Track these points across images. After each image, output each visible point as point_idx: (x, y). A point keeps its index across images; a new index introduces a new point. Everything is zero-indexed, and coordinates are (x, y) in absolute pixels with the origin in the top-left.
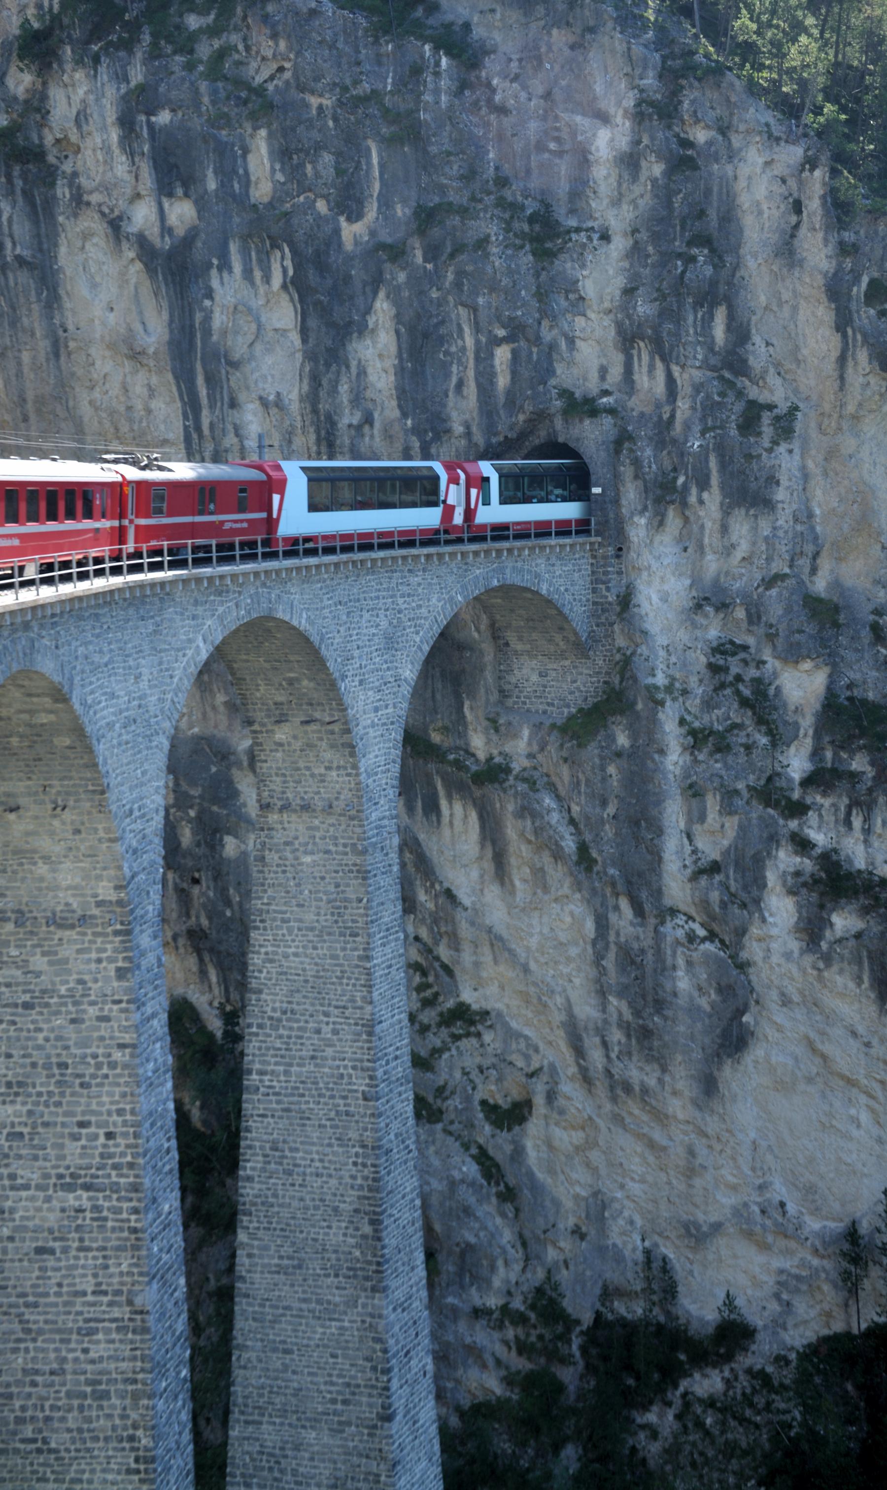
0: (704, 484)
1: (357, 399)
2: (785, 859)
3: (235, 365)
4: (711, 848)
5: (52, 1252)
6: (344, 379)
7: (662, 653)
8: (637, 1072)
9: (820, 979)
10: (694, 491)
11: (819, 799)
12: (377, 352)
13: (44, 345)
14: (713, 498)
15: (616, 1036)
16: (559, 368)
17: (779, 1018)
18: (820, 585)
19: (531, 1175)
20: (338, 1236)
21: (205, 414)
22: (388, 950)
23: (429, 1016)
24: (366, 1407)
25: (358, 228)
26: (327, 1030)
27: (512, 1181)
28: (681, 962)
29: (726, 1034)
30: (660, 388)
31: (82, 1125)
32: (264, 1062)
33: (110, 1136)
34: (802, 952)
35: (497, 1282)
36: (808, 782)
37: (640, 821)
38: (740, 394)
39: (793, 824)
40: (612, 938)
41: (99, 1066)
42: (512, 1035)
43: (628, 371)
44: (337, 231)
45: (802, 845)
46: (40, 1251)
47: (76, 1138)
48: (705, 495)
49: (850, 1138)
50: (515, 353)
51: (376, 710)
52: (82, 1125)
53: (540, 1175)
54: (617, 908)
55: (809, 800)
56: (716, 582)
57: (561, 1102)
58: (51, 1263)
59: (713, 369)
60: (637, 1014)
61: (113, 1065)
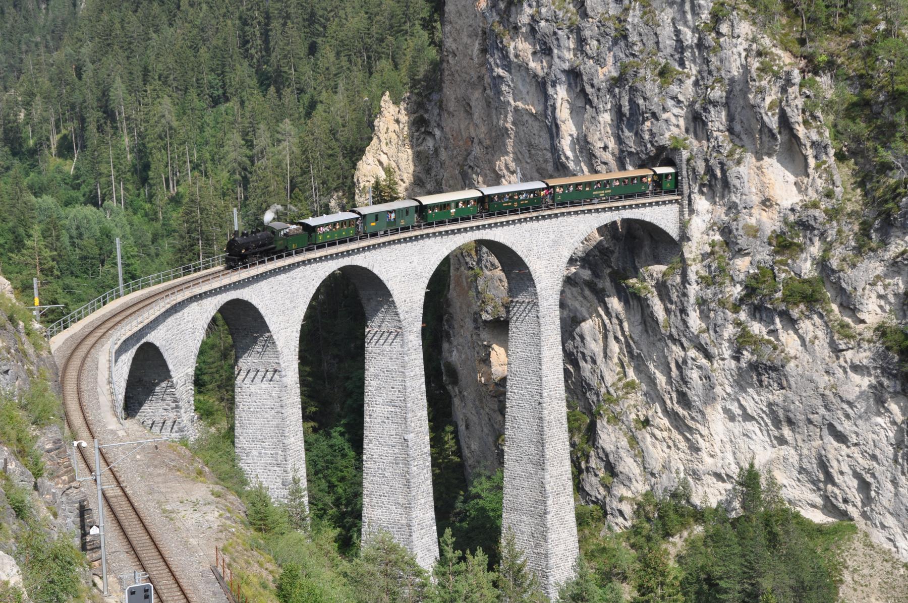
15: (674, 395)
16: (672, 128)
18: (753, 221)
19: (647, 448)
20: (532, 449)
23: (620, 384)
25: (605, 69)
35: (633, 488)
44: (597, 71)
50: (652, 123)
51: (547, 267)
53: (650, 447)
59: (722, 131)
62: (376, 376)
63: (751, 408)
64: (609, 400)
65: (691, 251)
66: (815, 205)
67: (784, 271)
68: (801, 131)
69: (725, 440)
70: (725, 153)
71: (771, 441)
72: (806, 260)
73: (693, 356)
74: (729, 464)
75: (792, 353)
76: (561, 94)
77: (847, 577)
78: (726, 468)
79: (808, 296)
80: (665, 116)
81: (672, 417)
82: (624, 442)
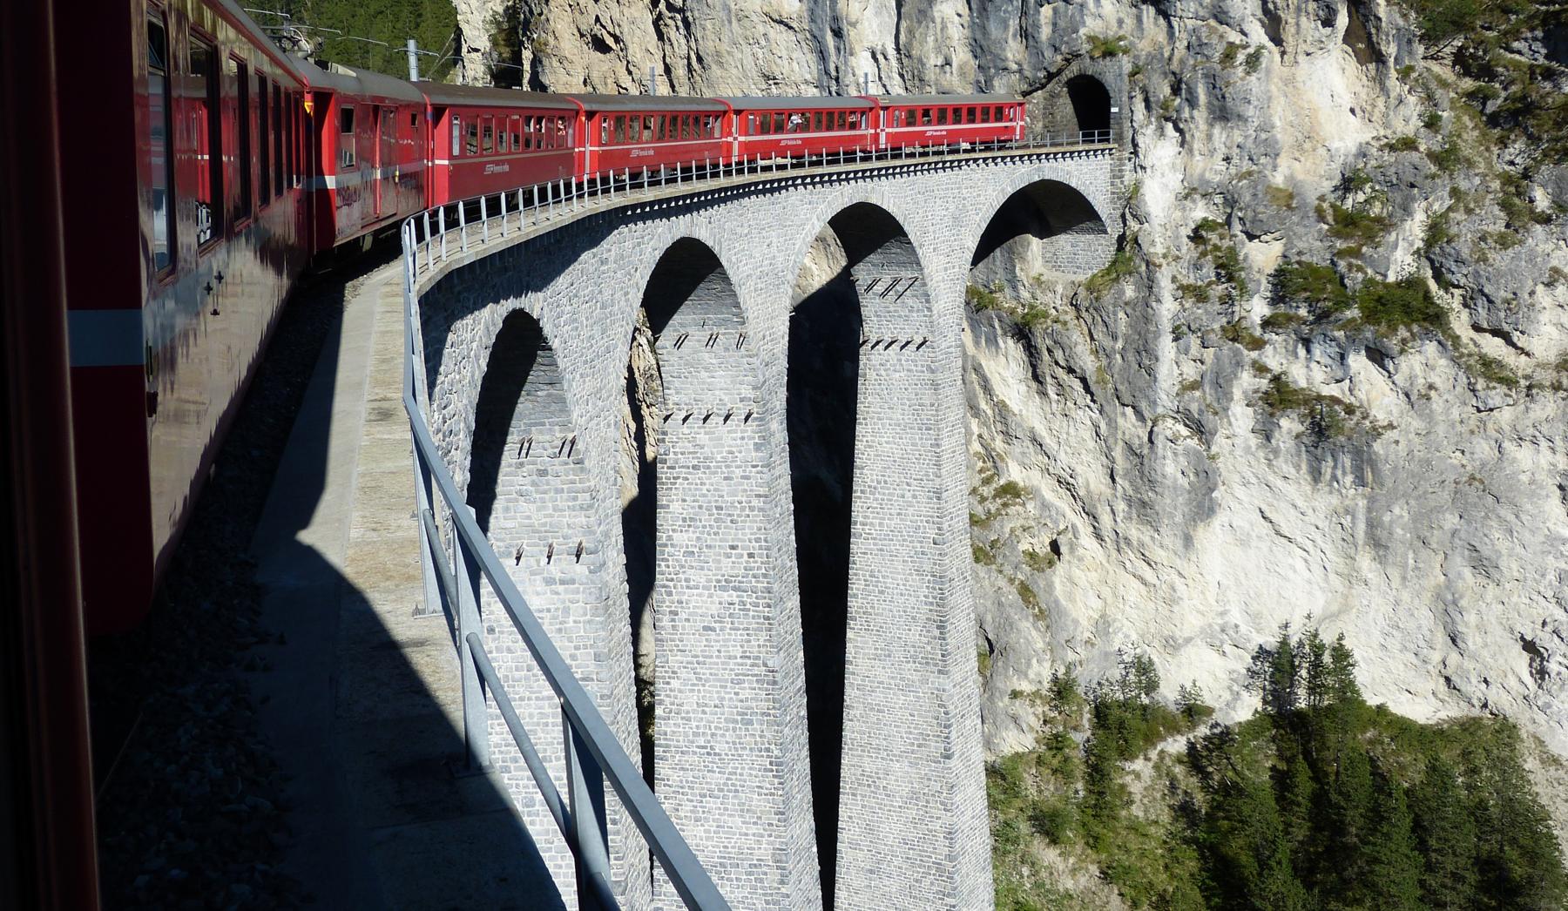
0: (1192, 102)
1: (942, 44)
2: (1246, 381)
3: (854, 25)
4: (1191, 371)
5: (713, 630)
6: (931, 32)
7: (1159, 229)
8: (1134, 532)
9: (1270, 465)
10: (1187, 109)
11: (1274, 336)
13: (723, 15)
14: (1201, 115)
15: (1121, 506)
16: (1089, 21)
17: (1240, 491)
18: (1278, 179)
19: (1057, 602)
20: (915, 635)
21: (833, 58)
22: (953, 440)
23: (987, 491)
24: (936, 747)
26: (908, 494)
27: (1044, 606)
28: (1169, 453)
29: (1200, 506)
30: (1162, 37)
31: (733, 547)
32: (866, 517)
33: (751, 555)
34: (1258, 447)
35: (1031, 675)
36: (1267, 324)
37: (1143, 350)
38: (1221, 37)
39: (1254, 354)
40: (1120, 436)
41: (743, 509)
42: (1045, 506)
43: (1139, 19)
45: (1260, 369)
46: (706, 628)
47: (728, 556)
48: (1195, 113)
49: (1286, 579)
50: (1055, 10)
52: (733, 547)
53: (1063, 602)
54: (1124, 414)
55: (1266, 337)
56: (1202, 175)
57: (1081, 551)
58: (713, 636)
60: (1136, 490)
61: (752, 509)
62: (689, 522)
63: (1287, 520)
66: (1408, 144)
67: (1360, 269)
69: (1224, 582)
70: (1217, 56)
71: (1326, 579)
72: (1396, 246)
73: (1169, 433)
74: (1237, 626)
75: (1382, 418)
78: (1231, 632)
81: (1109, 543)
82: (1012, 595)
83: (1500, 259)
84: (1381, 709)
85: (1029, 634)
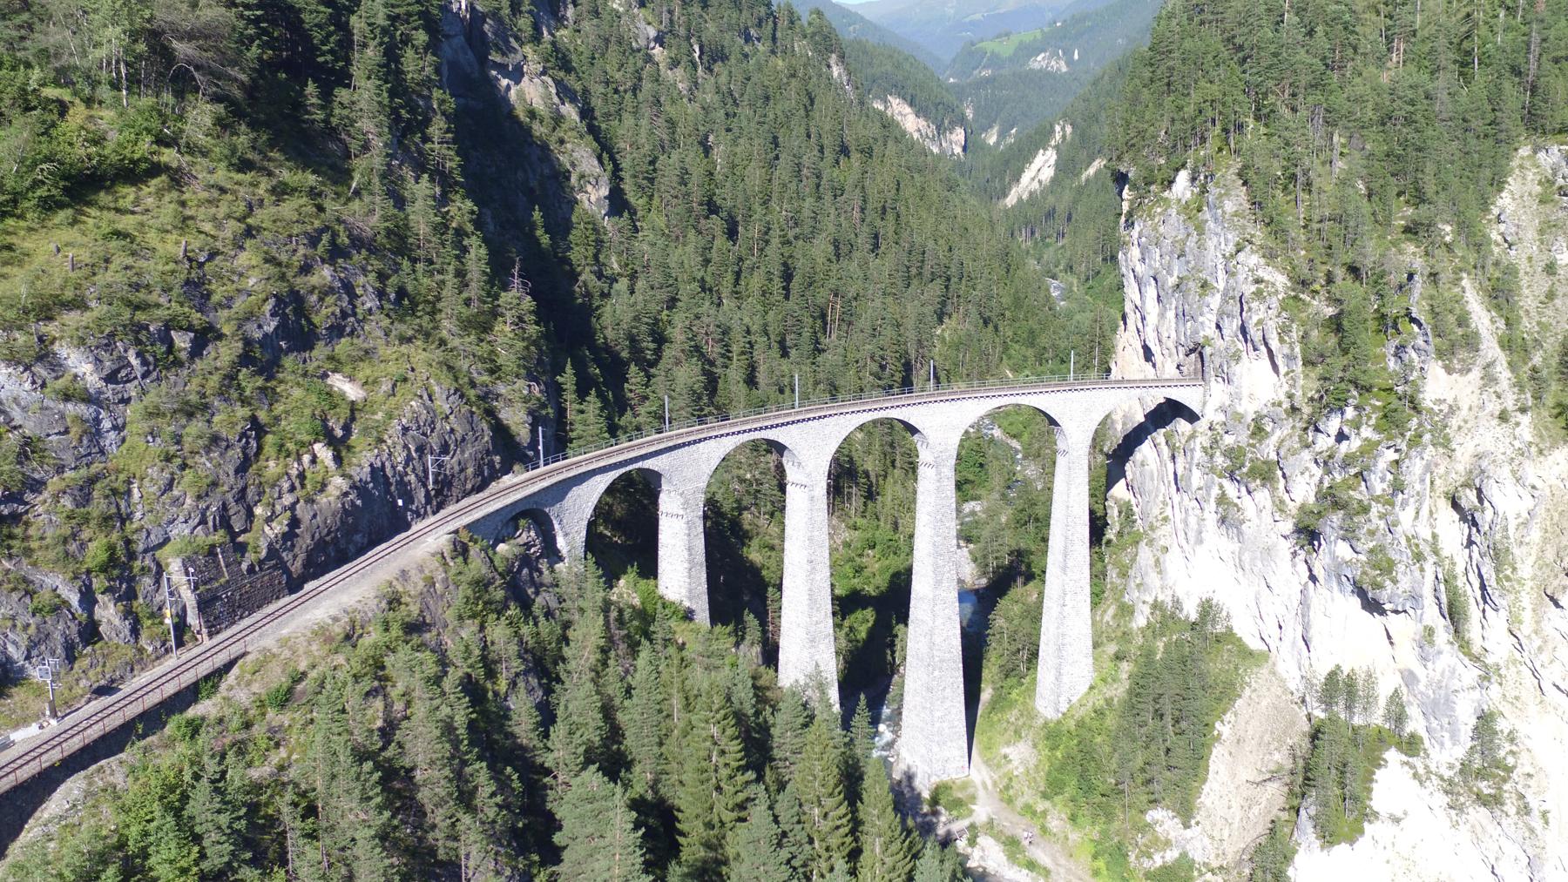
12: (1171, 314)
18: (1240, 410)
45: (1221, 487)
64: (1152, 528)
65: (1202, 425)
66: (1280, 405)
68: (1274, 344)
76: (1151, 292)
77: (1247, 691)
79: (1265, 473)
80: (1201, 319)
82: (1152, 561)
83: (1291, 459)
84: (1240, 639)
85: (1153, 579)
